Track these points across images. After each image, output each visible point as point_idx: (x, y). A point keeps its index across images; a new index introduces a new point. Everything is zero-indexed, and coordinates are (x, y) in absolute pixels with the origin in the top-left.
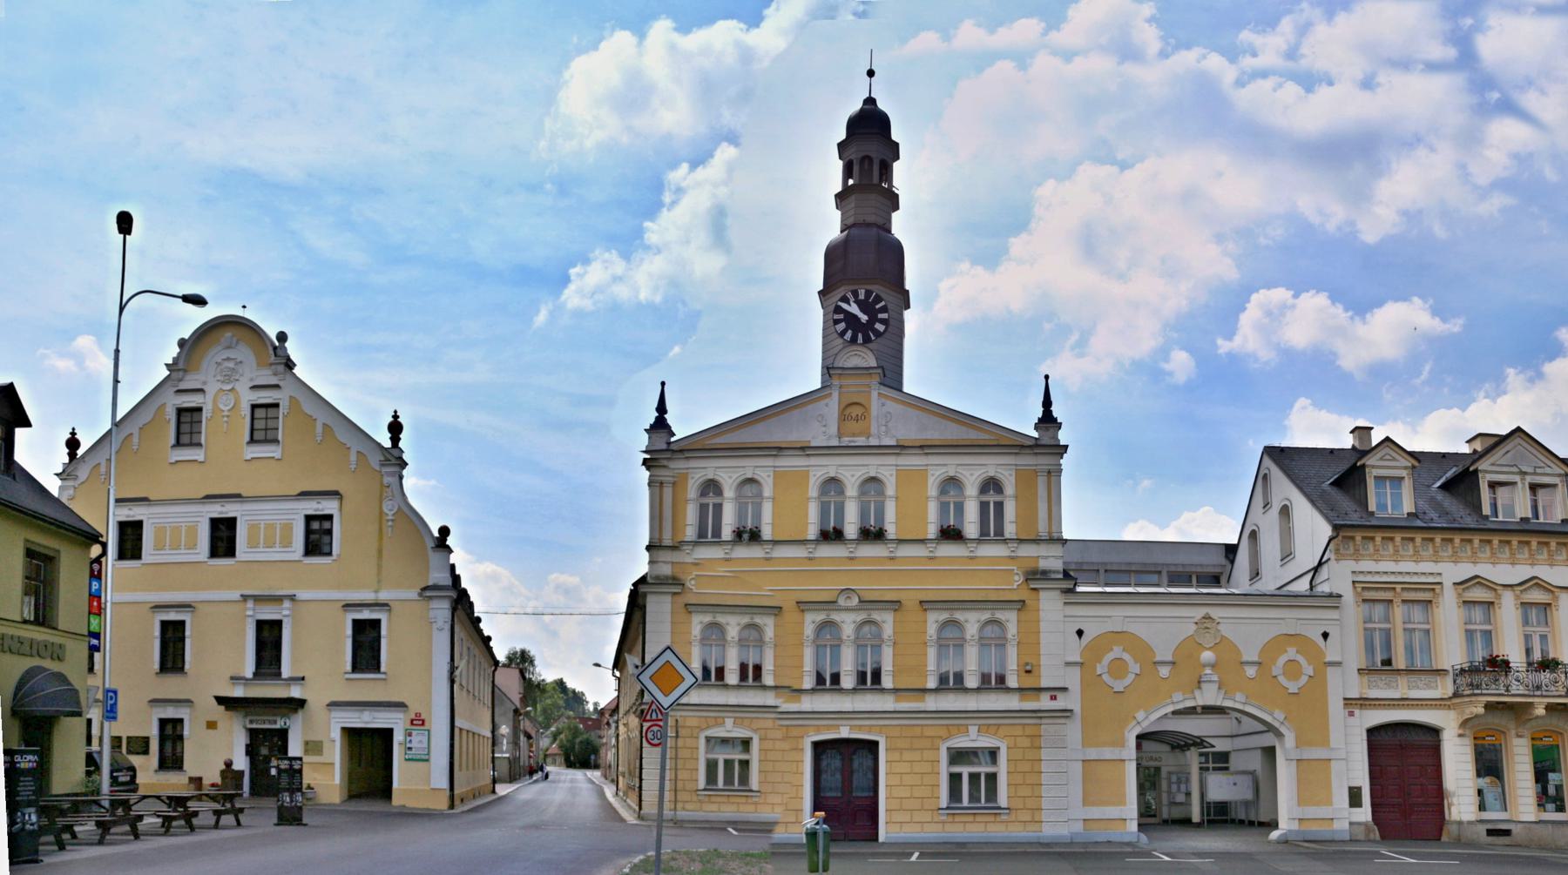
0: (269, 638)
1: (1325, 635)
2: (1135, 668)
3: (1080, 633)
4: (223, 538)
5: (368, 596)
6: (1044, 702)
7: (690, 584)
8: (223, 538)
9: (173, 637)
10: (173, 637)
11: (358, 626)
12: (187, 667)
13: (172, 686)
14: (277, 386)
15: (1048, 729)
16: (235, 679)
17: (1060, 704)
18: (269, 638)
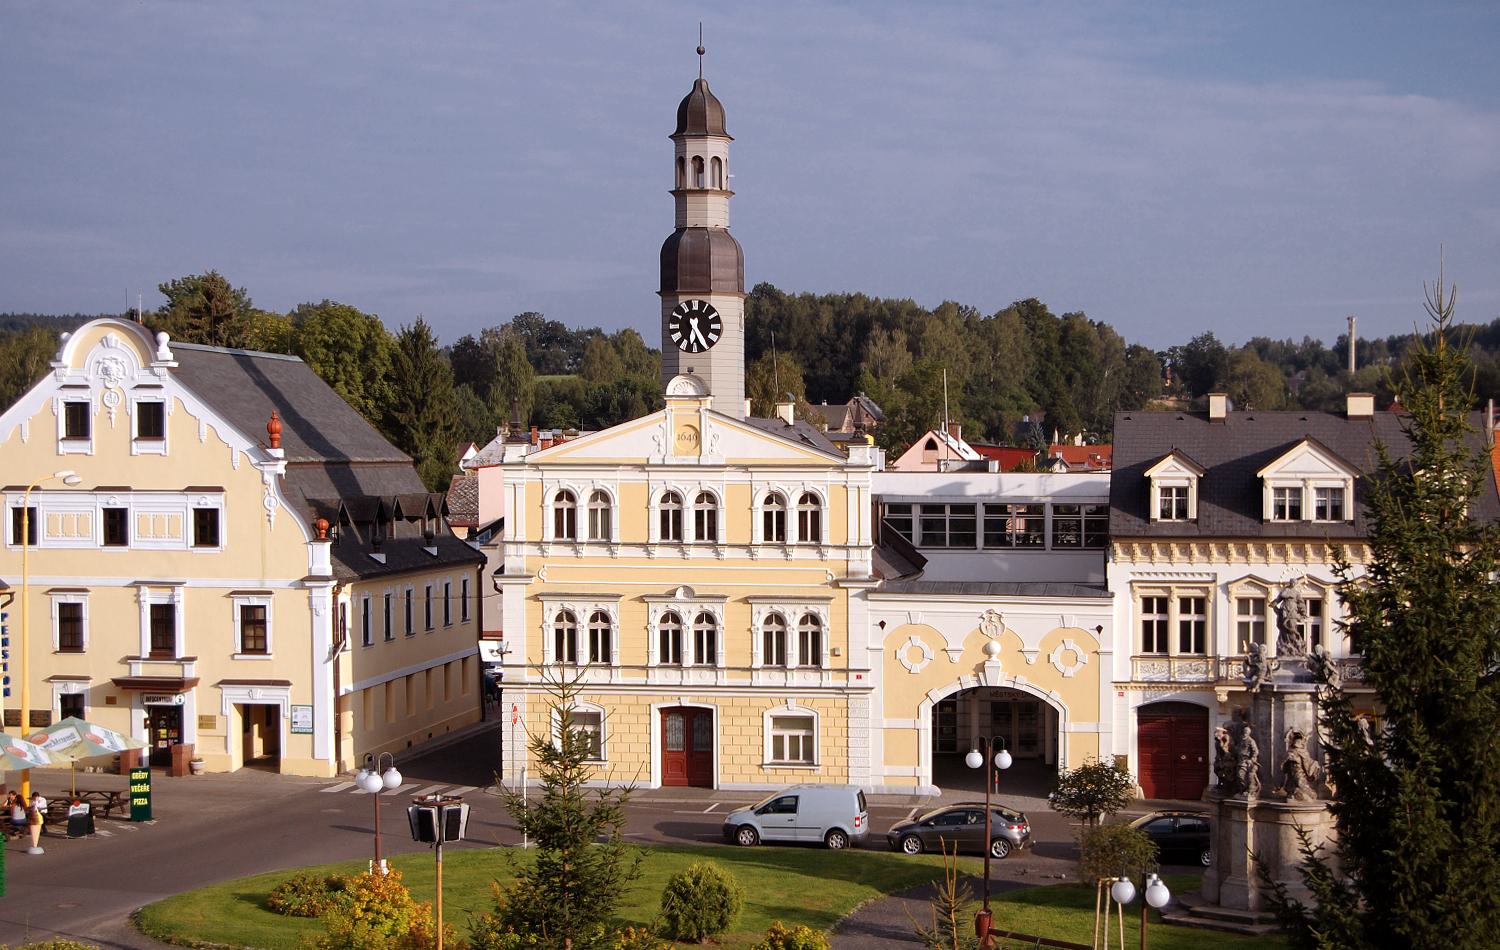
0: (163, 619)
1: (1099, 629)
2: (930, 653)
3: (882, 624)
4: (116, 527)
5: (252, 584)
6: (853, 682)
7: (544, 574)
8: (116, 527)
9: (70, 618)
10: (70, 618)
11: (247, 611)
12: (86, 646)
13: (70, 663)
14: (159, 387)
15: (855, 701)
16: (128, 660)
17: (867, 680)
18: (163, 619)
